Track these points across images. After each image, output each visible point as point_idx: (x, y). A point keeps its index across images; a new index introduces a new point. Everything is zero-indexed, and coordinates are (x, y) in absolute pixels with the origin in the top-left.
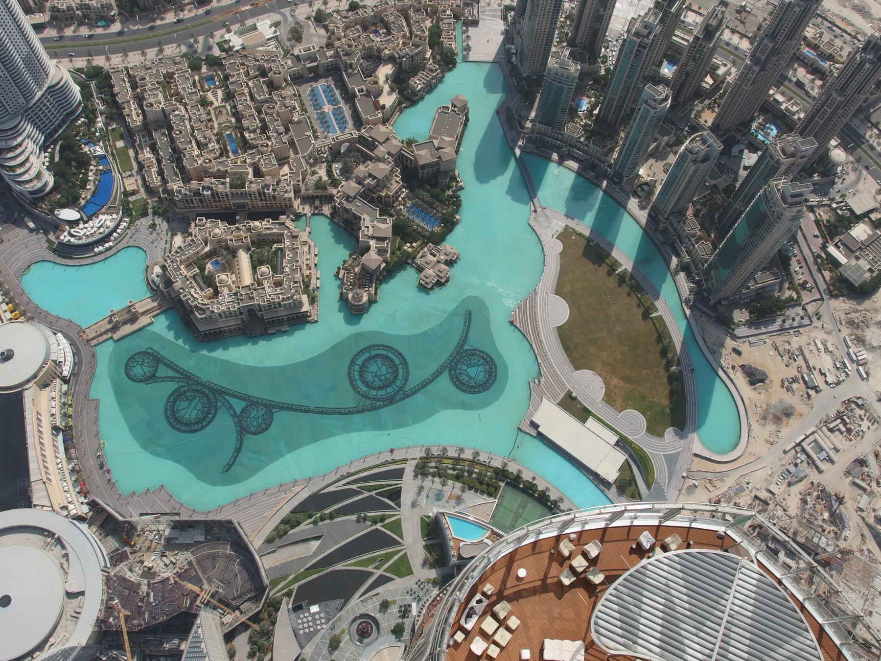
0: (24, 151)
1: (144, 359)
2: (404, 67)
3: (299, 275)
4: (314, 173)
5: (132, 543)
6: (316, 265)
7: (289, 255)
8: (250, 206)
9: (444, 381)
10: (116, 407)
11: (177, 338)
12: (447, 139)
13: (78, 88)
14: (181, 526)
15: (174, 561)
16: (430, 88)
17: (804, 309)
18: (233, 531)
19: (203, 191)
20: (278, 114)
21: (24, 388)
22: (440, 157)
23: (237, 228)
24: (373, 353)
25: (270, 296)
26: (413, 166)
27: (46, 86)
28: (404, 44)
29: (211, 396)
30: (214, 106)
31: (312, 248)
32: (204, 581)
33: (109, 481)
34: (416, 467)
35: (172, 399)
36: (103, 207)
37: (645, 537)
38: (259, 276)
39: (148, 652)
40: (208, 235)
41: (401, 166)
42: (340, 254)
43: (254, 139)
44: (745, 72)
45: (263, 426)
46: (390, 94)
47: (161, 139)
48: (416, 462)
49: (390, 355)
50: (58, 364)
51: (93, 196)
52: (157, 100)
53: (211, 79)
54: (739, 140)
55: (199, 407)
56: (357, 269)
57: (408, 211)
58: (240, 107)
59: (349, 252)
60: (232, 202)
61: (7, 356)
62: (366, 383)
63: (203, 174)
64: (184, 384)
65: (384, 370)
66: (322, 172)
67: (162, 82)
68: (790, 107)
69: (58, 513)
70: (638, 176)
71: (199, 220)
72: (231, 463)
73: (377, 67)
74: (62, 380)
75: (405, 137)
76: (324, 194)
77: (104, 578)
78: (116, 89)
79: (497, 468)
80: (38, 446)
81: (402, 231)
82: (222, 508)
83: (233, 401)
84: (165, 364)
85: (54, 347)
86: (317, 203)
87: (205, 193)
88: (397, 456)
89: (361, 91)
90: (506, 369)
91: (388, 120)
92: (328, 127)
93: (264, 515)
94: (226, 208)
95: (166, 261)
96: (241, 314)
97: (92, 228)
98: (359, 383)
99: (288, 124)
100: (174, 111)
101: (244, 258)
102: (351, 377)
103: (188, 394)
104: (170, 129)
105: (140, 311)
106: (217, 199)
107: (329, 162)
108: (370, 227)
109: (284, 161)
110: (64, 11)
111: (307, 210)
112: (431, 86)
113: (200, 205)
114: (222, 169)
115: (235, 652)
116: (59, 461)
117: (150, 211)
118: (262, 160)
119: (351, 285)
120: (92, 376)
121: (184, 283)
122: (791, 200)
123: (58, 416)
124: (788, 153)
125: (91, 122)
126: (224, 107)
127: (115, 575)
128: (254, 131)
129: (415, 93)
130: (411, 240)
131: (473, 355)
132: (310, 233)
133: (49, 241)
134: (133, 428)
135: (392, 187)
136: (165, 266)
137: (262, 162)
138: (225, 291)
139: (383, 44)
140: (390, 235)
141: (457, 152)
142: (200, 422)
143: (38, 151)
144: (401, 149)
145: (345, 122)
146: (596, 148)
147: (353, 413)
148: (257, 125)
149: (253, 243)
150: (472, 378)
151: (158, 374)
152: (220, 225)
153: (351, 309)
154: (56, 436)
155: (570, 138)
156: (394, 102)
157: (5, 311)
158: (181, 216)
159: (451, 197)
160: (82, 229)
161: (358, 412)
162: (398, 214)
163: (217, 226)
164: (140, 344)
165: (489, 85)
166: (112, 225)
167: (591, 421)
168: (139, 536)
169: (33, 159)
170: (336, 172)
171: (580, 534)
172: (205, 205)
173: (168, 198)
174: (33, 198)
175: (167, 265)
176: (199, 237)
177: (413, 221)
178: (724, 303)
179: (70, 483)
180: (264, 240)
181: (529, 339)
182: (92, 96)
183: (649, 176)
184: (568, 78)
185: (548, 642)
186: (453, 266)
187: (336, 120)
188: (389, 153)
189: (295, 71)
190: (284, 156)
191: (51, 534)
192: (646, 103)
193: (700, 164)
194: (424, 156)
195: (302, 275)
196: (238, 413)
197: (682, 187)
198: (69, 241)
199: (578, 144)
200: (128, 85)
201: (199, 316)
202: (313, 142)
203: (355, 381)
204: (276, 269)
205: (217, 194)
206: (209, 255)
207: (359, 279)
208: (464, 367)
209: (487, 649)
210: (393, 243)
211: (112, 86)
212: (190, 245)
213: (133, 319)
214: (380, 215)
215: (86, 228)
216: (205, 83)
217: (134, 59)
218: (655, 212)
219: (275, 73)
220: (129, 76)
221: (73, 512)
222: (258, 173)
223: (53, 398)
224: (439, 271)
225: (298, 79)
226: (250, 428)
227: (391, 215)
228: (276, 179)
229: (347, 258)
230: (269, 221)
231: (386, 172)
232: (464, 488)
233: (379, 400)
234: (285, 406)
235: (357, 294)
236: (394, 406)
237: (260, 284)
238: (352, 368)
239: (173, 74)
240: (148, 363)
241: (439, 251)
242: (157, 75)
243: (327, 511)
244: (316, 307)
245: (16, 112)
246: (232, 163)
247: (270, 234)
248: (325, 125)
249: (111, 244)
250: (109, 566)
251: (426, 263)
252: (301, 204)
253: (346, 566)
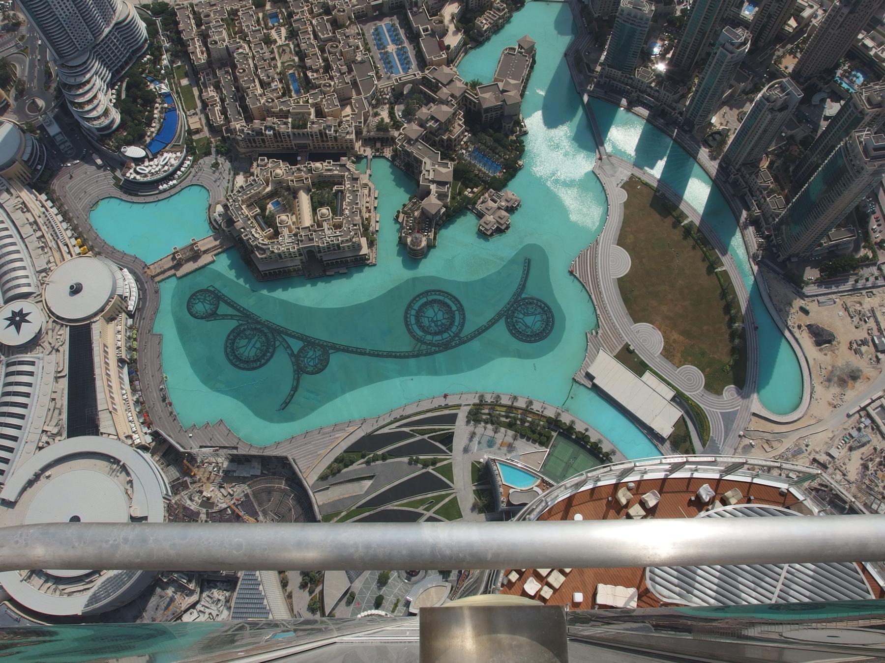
0: (92, 88)
1: (205, 297)
2: (470, 6)
3: (358, 218)
4: (376, 114)
5: (192, 474)
6: (375, 208)
7: (349, 197)
8: (312, 147)
9: (501, 327)
10: (178, 343)
11: (238, 277)
12: (513, 82)
13: (144, 25)
14: (237, 460)
15: (232, 493)
16: (497, 28)
17: (879, 269)
18: (288, 467)
19: (265, 131)
20: (341, 54)
21: (92, 320)
22: (504, 101)
23: (298, 169)
24: (430, 298)
25: (329, 237)
26: (476, 110)
27: (114, 22)
29: (270, 335)
30: (278, 44)
31: (372, 191)
32: (259, 513)
33: (171, 413)
34: (469, 413)
35: (232, 337)
36: (167, 145)
37: (705, 489)
38: (319, 218)
39: (206, 576)
40: (269, 175)
41: (464, 109)
42: (400, 197)
43: (317, 78)
44: (833, 14)
45: (319, 366)
46: (455, 33)
47: (225, 78)
48: (469, 408)
49: (447, 300)
50: (124, 299)
51: (157, 134)
52: (222, 38)
53: (275, 16)
54: (821, 88)
55: (258, 345)
56: (416, 214)
57: (470, 155)
58: (303, 46)
59: (409, 196)
60: (293, 142)
61: (76, 290)
62: (422, 328)
63: (266, 113)
64: (244, 323)
65: (440, 316)
66: (384, 114)
67: (226, 19)
68: (879, 53)
69: (123, 442)
70: (711, 124)
71: (261, 160)
72: (288, 401)
73: (443, 6)
74: (128, 315)
75: (469, 79)
76: (385, 136)
77: (166, 506)
78: (181, 26)
79: (550, 417)
80: (105, 377)
81: (463, 176)
82: (278, 444)
83: (291, 341)
84: (226, 302)
85: (120, 283)
86: (378, 145)
87: (267, 132)
88: (451, 401)
89: (426, 30)
90: (563, 318)
91: (452, 61)
92: (392, 67)
93: (319, 453)
94: (288, 148)
95: (228, 200)
96: (300, 255)
97: (157, 166)
98: (415, 327)
99: (350, 64)
100: (238, 49)
101: (304, 199)
102: (407, 322)
103: (248, 333)
104: (234, 67)
105: (203, 249)
106: (279, 139)
107: (391, 103)
108: (431, 171)
109: (346, 102)
111: (369, 152)
112: (497, 26)
113: (262, 144)
114: (285, 109)
115: (287, 582)
116: (124, 392)
117: (213, 150)
119: (410, 229)
120: (156, 311)
121: (245, 222)
122: (873, 153)
123: (123, 349)
124: (874, 102)
125: (157, 59)
126: (288, 45)
127: (176, 503)
128: (317, 71)
129: (481, 33)
130: (472, 185)
131: (530, 303)
132: (370, 175)
133: (115, 178)
134: (194, 364)
135: (455, 131)
136: (227, 205)
137: (324, 102)
138: (286, 232)
140: (451, 179)
141: (522, 95)
142: (258, 360)
143: (105, 88)
144: (465, 92)
145: (409, 62)
146: (667, 94)
147: (407, 357)
148: (320, 64)
149: (314, 184)
150: (529, 327)
151: (219, 312)
152: (281, 165)
153: (410, 253)
154: (122, 368)
155: (640, 83)
156: (459, 43)
157: (74, 246)
158: (243, 156)
159: (515, 142)
160: (147, 167)
161: (413, 356)
162: (459, 159)
163: (278, 166)
164: (203, 282)
165: (559, 26)
166: (175, 163)
167: (647, 375)
168: (198, 467)
169: (101, 96)
170: (398, 114)
171: (639, 483)
175: (229, 205)
176: (261, 177)
177: (475, 166)
178: (793, 260)
179: (134, 413)
180: (324, 182)
181: (588, 289)
182: (158, 32)
183: (721, 124)
184: (641, 19)
185: (601, 587)
186: (514, 213)
187: (400, 60)
188: (452, 96)
189: (359, 8)
191: (116, 461)
192: (723, 47)
193: (777, 113)
194: (488, 99)
195: (362, 217)
196: (296, 353)
197: (757, 137)
198: (135, 178)
199: (649, 90)
200: (193, 21)
201: (259, 256)
202: (376, 82)
203: (412, 325)
204: (336, 211)
205: (279, 134)
206: (271, 196)
207: (419, 223)
208: (521, 316)
209: (541, 589)
210: (454, 188)
212: (252, 185)
213: (195, 255)
214: (442, 159)
215: (151, 166)
216: (269, 21)
218: (726, 163)
219: (339, 11)
220: (194, 13)
221: (138, 441)
222: (320, 114)
223: (119, 332)
224: (499, 217)
225: (362, 17)
226: (307, 368)
227: (453, 160)
228: (338, 120)
229: (407, 202)
230: (329, 163)
231: (449, 116)
232: (516, 436)
233: (434, 345)
234: (342, 348)
235: (416, 238)
236: (449, 352)
237: (320, 225)
238: (409, 312)
239: (237, 10)
240: (210, 301)
241: (500, 197)
242: (221, 12)
243: (380, 452)
244: (374, 251)
245: (84, 49)
246: (294, 103)
247: (331, 176)
248: (389, 66)
249: (175, 182)
250: (170, 494)
251: (486, 209)
252: (362, 145)
253: (396, 506)
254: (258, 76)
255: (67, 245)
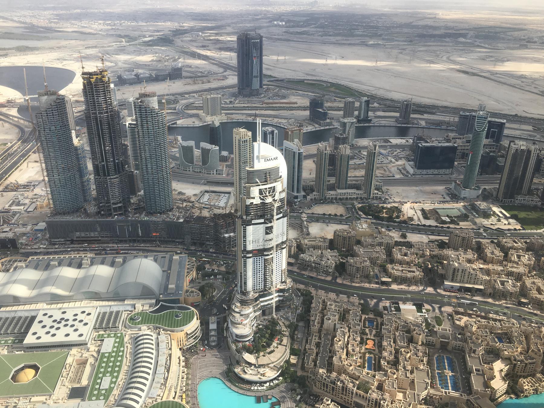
28: (521, 353)
58: (385, 343)
60: (354, 399)
73: (494, 361)
78: (313, 305)
106: (344, 393)
110: (306, 261)
113: (331, 391)
118: (387, 381)
139: (503, 347)
172: (334, 393)
173: (313, 377)
174: (236, 340)
190: (403, 387)
200: (321, 306)
205: (346, 389)
211: (311, 303)
217: (332, 295)
220: (324, 301)
222: (380, 387)
239: (350, 310)
242: (340, 307)
254: (347, 347)
255: (176, 392)
